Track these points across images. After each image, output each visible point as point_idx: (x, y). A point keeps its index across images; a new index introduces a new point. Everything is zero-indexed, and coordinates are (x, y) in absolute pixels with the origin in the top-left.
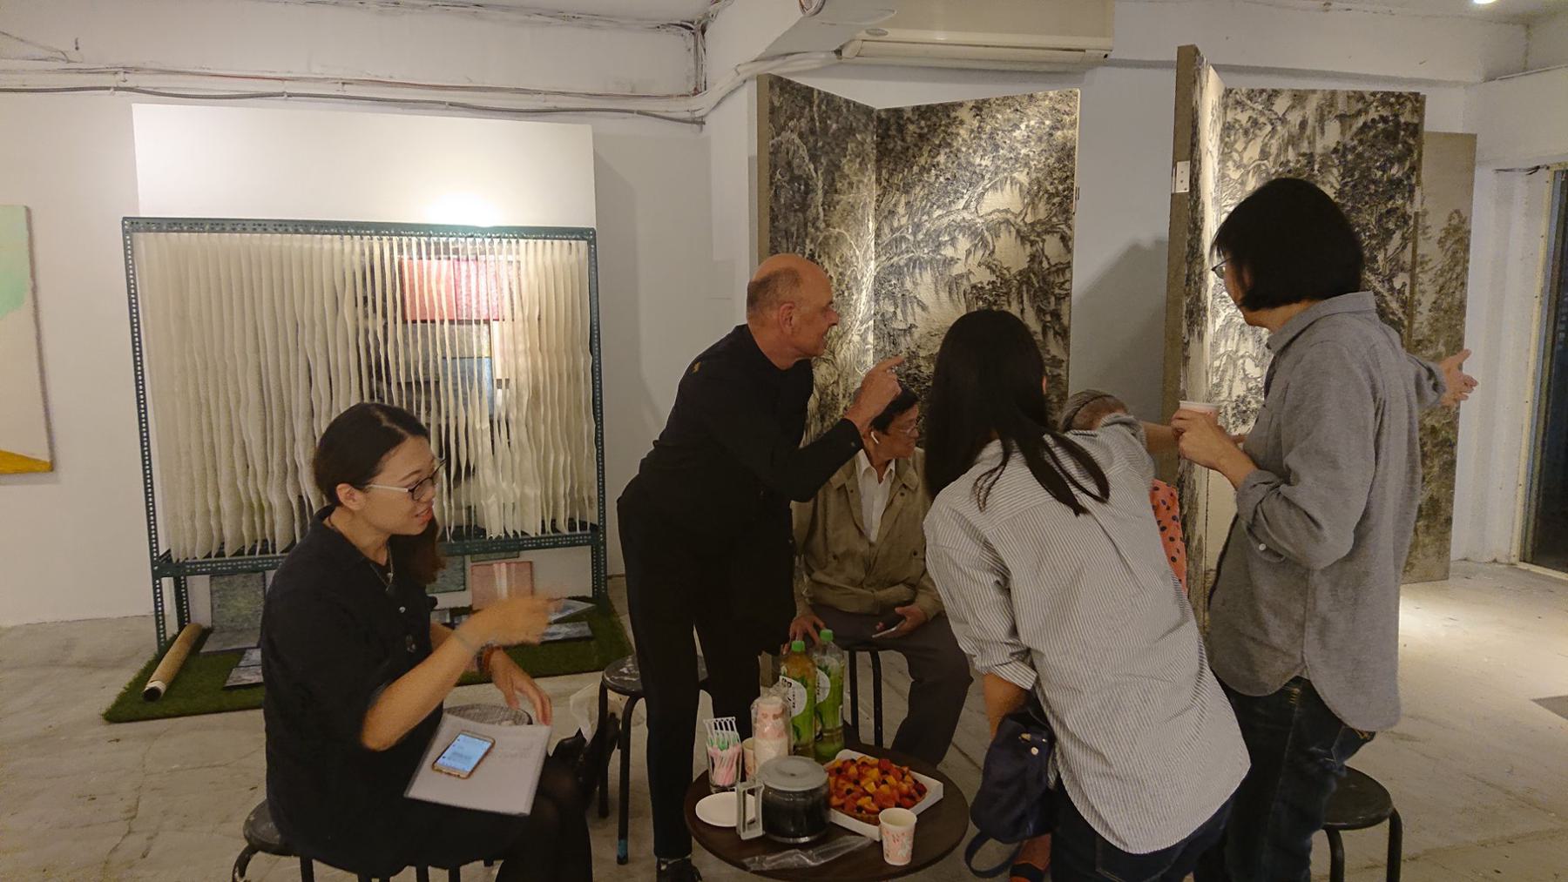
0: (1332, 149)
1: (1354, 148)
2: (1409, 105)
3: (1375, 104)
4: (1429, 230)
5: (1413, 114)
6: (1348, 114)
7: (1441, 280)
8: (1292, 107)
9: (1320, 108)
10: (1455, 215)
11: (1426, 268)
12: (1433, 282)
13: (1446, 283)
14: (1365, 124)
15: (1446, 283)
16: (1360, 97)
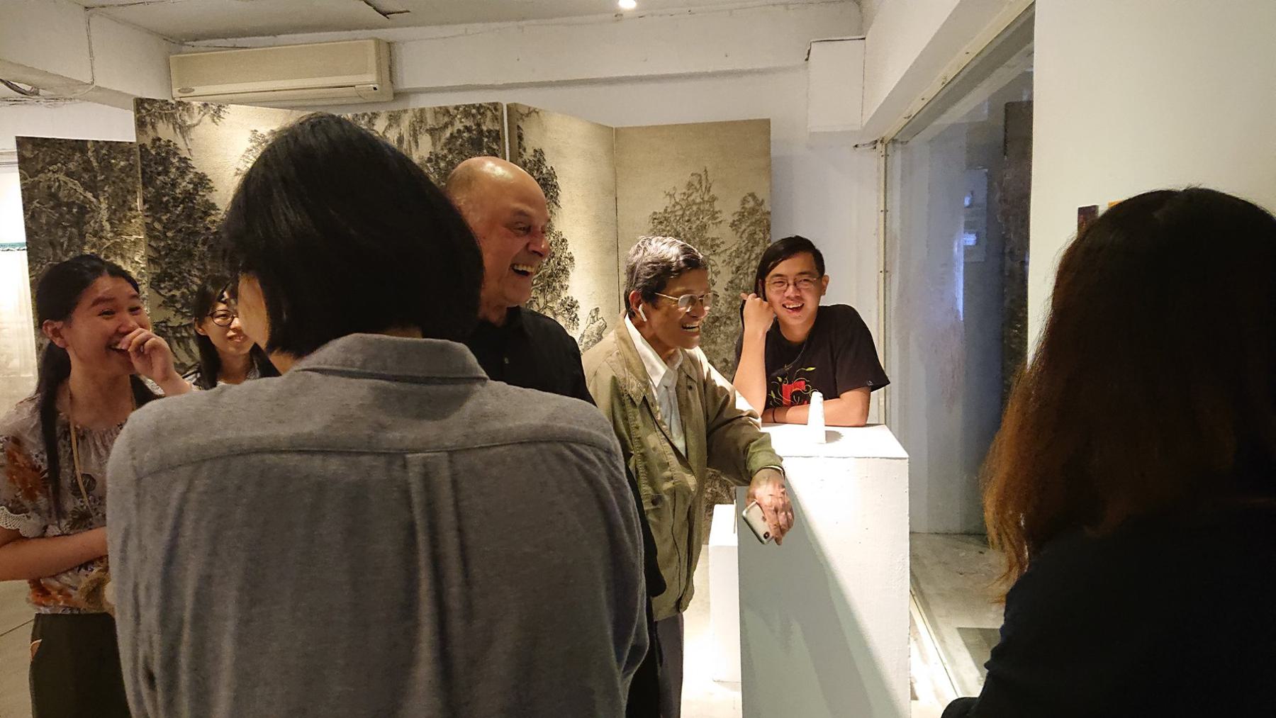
0: (426, 159)
1: (445, 156)
2: (489, 114)
3: (458, 116)
4: (716, 215)
5: (494, 122)
6: (437, 127)
7: (737, 262)
8: (390, 126)
9: (412, 125)
10: (750, 199)
11: (718, 250)
12: (728, 263)
13: (743, 263)
14: (451, 134)
15: (743, 263)
16: (446, 111)
